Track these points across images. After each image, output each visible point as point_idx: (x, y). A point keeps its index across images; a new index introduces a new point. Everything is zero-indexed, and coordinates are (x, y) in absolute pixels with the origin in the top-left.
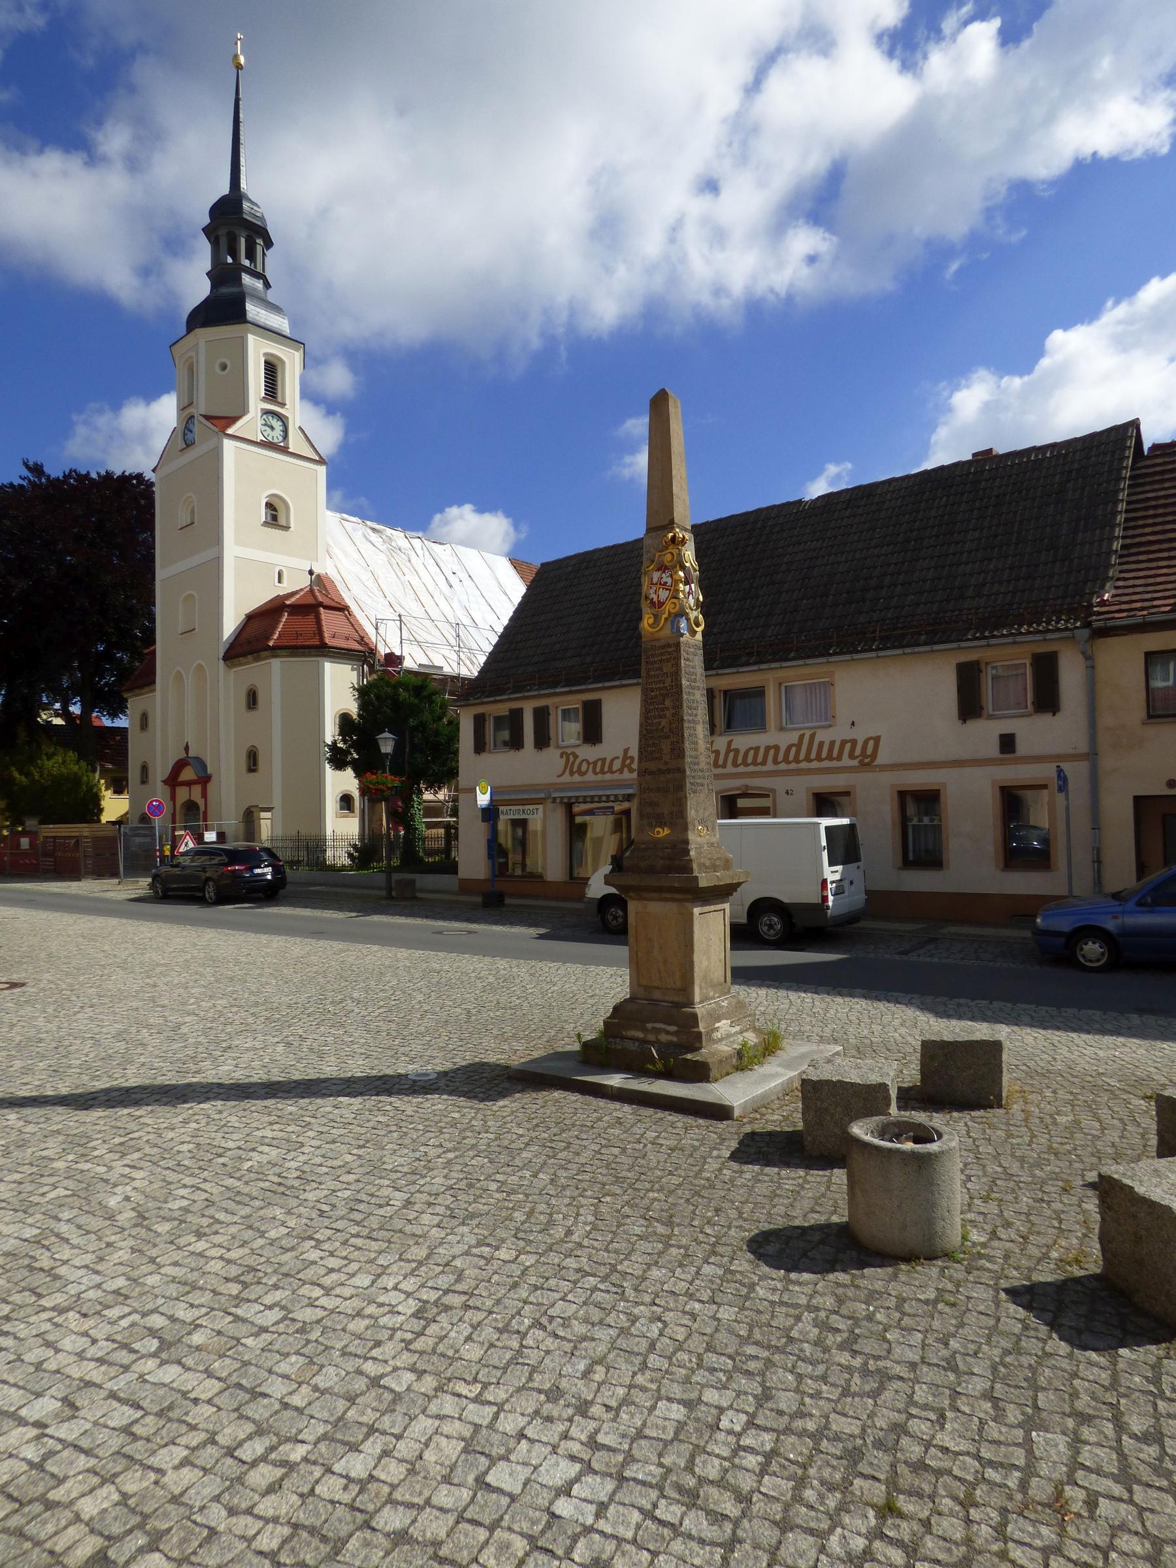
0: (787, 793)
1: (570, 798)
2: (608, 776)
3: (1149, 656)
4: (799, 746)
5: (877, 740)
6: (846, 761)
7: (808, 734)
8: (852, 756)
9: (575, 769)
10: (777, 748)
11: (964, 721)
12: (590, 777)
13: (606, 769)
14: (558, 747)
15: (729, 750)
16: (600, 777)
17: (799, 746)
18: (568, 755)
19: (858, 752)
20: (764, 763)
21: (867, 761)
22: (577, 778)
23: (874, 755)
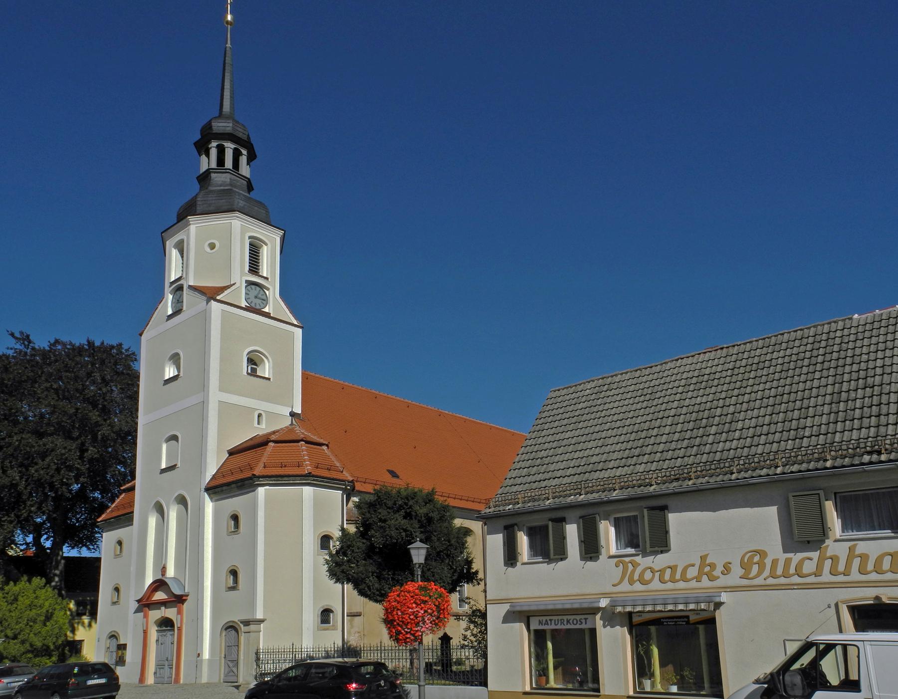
2: (681, 585)
9: (636, 577)
12: (656, 585)
13: (678, 576)
16: (670, 585)
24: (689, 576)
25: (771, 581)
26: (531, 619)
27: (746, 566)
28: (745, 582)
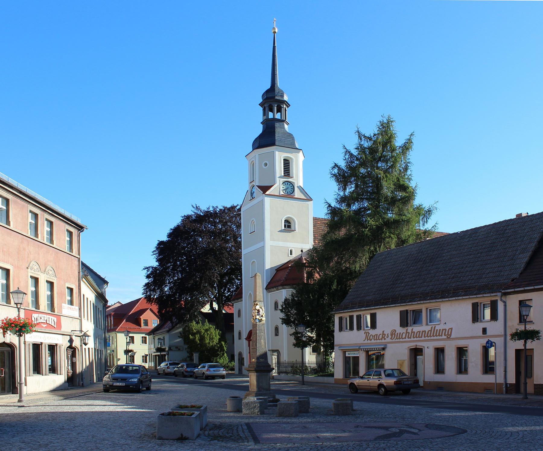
0: (428, 348)
1: (368, 349)
2: (378, 341)
3: (520, 302)
4: (431, 331)
5: (452, 329)
6: (444, 337)
7: (434, 326)
8: (445, 335)
10: (425, 331)
11: (474, 323)
12: (373, 341)
14: (364, 329)
15: (412, 332)
16: (376, 341)
17: (431, 331)
18: (367, 333)
19: (446, 334)
20: (421, 337)
21: (449, 337)
22: (369, 341)
23: (451, 335)
24: (380, 339)
25: (397, 340)
26: (346, 352)
27: (392, 335)
28: (391, 340)
